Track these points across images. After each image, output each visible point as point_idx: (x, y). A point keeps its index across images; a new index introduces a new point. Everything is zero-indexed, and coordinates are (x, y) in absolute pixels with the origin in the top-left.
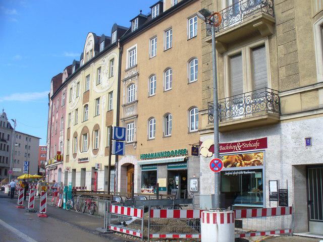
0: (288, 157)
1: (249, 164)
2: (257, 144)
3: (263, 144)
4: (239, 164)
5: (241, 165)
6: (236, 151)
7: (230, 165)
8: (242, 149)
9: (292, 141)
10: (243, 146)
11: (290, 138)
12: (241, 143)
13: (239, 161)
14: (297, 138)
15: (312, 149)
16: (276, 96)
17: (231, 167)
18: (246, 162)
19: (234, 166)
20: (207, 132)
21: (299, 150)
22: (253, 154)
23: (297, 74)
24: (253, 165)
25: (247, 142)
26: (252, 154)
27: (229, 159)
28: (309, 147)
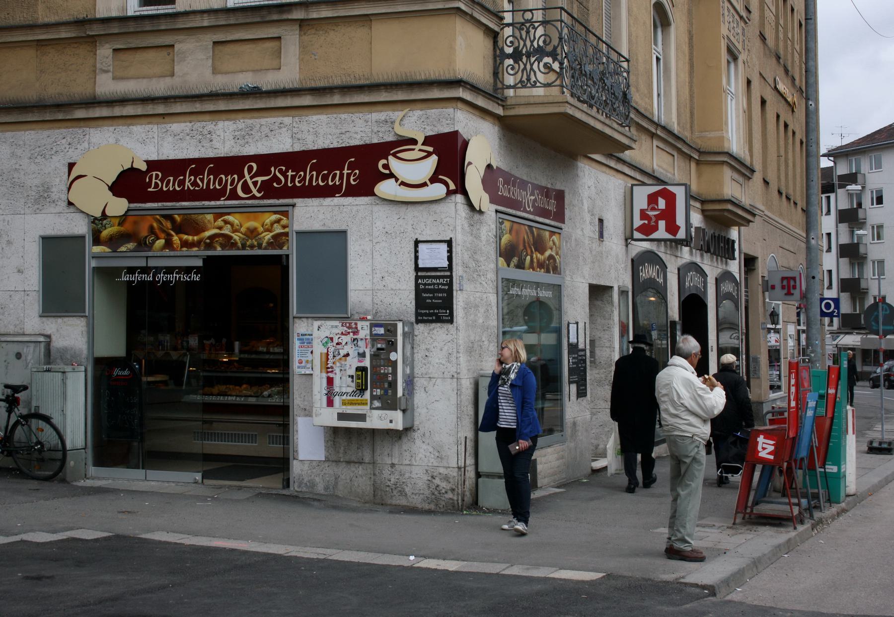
1: (197, 244)
4: (160, 242)
5: (169, 244)
13: (163, 235)
18: (185, 237)
22: (210, 217)
24: (209, 246)
27: (128, 227)
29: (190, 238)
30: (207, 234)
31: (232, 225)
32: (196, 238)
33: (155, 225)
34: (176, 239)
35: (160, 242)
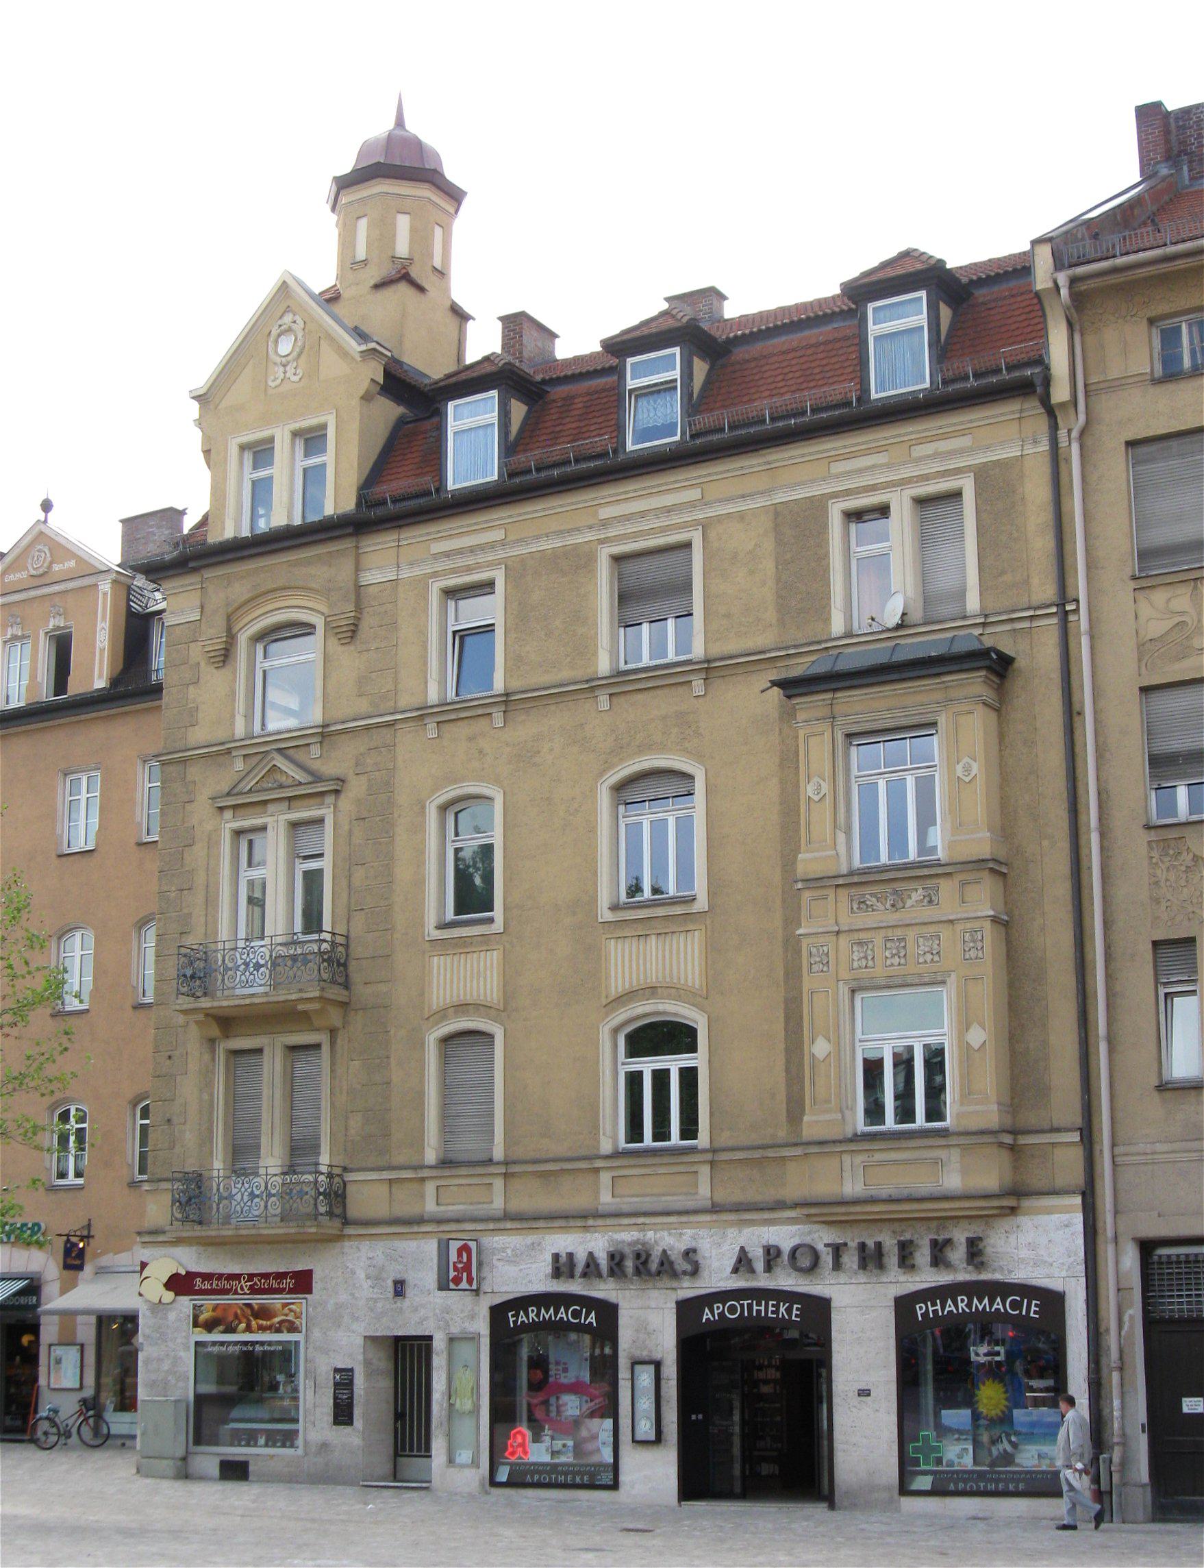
0: (356, 1319)
2: (288, 1283)
3: (303, 1282)
4: (243, 1326)
6: (236, 1293)
7: (221, 1328)
8: (254, 1290)
9: (366, 1284)
10: (255, 1284)
11: (363, 1276)
12: (251, 1276)
13: (245, 1320)
14: (376, 1278)
15: (406, 1303)
16: (337, 1179)
17: (225, 1332)
18: (261, 1322)
19: (231, 1330)
21: (379, 1305)
23: (387, 1135)
24: (278, 1331)
25: (266, 1276)
26: (275, 1302)
27: (219, 1313)
28: (399, 1302)
29: (264, 1323)
30: (277, 1320)
31: (295, 1313)
33: (239, 1312)
34: (254, 1323)
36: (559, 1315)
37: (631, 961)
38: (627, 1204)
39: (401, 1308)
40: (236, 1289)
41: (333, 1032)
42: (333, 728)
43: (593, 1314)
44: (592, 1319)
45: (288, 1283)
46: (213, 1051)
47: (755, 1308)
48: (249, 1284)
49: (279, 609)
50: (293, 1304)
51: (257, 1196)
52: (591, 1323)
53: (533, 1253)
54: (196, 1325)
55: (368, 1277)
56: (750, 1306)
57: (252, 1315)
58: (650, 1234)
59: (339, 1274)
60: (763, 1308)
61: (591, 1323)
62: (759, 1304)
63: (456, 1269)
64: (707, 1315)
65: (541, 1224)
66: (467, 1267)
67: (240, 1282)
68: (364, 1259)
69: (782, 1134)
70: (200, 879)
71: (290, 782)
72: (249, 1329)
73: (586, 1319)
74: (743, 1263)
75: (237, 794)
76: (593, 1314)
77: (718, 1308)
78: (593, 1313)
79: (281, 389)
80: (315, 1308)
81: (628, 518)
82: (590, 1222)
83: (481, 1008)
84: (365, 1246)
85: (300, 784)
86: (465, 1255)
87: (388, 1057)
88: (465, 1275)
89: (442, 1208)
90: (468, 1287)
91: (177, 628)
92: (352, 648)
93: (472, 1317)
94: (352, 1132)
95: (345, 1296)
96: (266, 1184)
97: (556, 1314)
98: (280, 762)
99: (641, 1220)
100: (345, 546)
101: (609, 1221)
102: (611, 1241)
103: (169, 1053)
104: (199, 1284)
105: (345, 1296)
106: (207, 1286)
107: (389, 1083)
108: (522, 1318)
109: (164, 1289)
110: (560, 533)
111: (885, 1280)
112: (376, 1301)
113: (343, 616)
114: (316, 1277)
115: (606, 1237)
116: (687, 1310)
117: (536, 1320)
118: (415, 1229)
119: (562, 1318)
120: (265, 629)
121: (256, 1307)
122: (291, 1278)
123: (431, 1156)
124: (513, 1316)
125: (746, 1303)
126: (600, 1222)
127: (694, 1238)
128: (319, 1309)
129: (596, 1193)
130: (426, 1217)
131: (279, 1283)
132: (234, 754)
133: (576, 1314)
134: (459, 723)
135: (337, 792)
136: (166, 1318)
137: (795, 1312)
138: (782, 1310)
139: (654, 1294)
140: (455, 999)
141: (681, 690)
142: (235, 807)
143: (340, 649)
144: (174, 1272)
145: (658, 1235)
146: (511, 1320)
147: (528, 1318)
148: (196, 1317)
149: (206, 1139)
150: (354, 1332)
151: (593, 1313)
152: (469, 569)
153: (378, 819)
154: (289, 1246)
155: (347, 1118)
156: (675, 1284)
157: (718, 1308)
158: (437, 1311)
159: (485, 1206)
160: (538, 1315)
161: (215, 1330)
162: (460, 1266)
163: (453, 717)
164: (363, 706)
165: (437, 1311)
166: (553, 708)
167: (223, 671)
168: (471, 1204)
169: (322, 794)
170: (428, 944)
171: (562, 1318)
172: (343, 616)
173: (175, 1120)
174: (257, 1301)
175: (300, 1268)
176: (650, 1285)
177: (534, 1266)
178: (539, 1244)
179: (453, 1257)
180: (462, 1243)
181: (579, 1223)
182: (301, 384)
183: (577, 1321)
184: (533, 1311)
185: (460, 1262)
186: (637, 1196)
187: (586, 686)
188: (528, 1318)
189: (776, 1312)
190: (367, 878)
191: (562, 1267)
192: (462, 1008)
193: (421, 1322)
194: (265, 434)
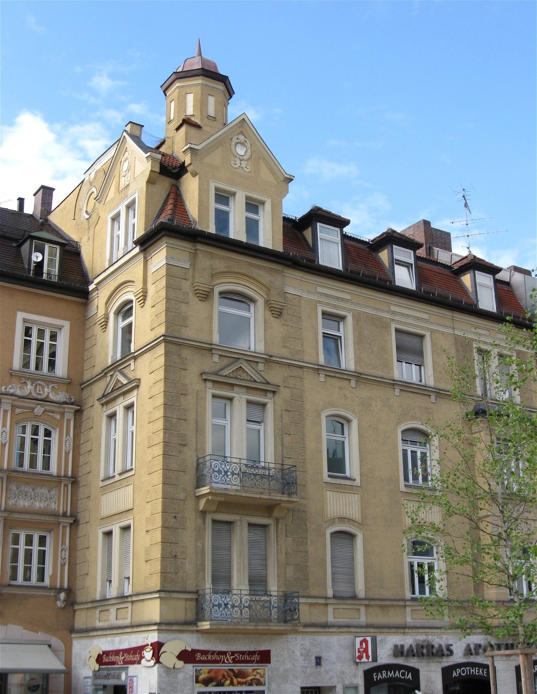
0: (296, 677)
2: (256, 657)
4: (228, 682)
6: (224, 662)
7: (214, 683)
8: (235, 661)
9: (301, 659)
12: (233, 653)
13: (229, 679)
14: (306, 655)
15: (322, 669)
18: (239, 680)
20: (175, 628)
21: (308, 670)
23: (307, 579)
24: (251, 684)
25: (243, 653)
26: (248, 668)
27: (212, 675)
28: (318, 667)
30: (249, 678)
31: (260, 674)
32: (244, 680)
33: (225, 673)
34: (235, 680)
35: (228, 682)
36: (396, 675)
37: (340, 506)
38: (418, 623)
39: (320, 672)
40: (224, 661)
41: (277, 520)
42: (274, 359)
43: (410, 674)
44: (410, 676)
45: (256, 657)
46: (204, 519)
47: (471, 671)
48: (232, 657)
49: (246, 286)
50: (259, 669)
51: (247, 607)
52: (409, 678)
53: (382, 645)
54: (197, 681)
55: (301, 655)
56: (470, 670)
57: (234, 676)
58: (430, 637)
59: (286, 653)
60: (474, 671)
61: (409, 678)
62: (473, 669)
63: (359, 651)
64: (454, 674)
65: (386, 630)
66: (366, 650)
67: (226, 656)
68: (299, 645)
69: (473, 595)
70: (192, 416)
71: (249, 378)
72: (232, 684)
73: (407, 676)
74: (468, 651)
75: (220, 375)
76: (410, 674)
77: (458, 671)
78: (410, 674)
79: (235, 170)
80: (272, 671)
81: (403, 315)
82: (407, 630)
83: (351, 521)
84: (299, 637)
85: (255, 381)
86: (364, 644)
87: (306, 538)
88: (364, 654)
89: (336, 620)
90: (366, 660)
91: (174, 267)
92: (278, 320)
93: (355, 676)
94: (288, 575)
95: (289, 665)
96: (241, 599)
97: (395, 674)
98: (246, 366)
99: (426, 630)
100: (279, 269)
101: (414, 631)
102: (415, 640)
103: (174, 515)
104: (198, 656)
105: (289, 665)
106: (204, 658)
107: (307, 552)
108: (380, 676)
109: (176, 659)
110: (375, 309)
111: (511, 659)
112: (306, 668)
113: (280, 304)
114: (272, 654)
115: (413, 638)
116: (447, 672)
117: (386, 677)
118: (327, 630)
119: (397, 676)
120: (241, 292)
121: (236, 671)
122: (258, 654)
123: (330, 593)
124: (375, 675)
125: (468, 668)
126: (410, 631)
127: (446, 639)
128: (275, 672)
129: (405, 616)
130: (329, 624)
131: (250, 658)
132: (213, 352)
133: (403, 674)
134: (334, 379)
135: (274, 392)
136: (177, 678)
137: (485, 672)
138: (481, 671)
139: (433, 664)
140: (335, 515)
141: (426, 397)
142: (214, 382)
143: (272, 318)
144: (184, 649)
145: (433, 638)
146: (375, 677)
147: (382, 676)
148: (197, 677)
149: (201, 568)
150: (295, 685)
151: (410, 674)
152: (335, 307)
153: (297, 413)
154: (256, 636)
155: (285, 568)
156: (440, 660)
157: (458, 671)
158: (338, 673)
159: (357, 620)
160: (387, 675)
161: (210, 685)
162: (361, 650)
163: (333, 375)
164: (285, 352)
165: (338, 673)
166: (376, 386)
167: (203, 303)
168: (350, 618)
169: (266, 391)
170: (324, 484)
171: (397, 676)
172: (280, 304)
173: (179, 556)
174: (237, 667)
175: (263, 648)
176: (431, 661)
177: (382, 650)
178: (384, 640)
179: (358, 646)
180: (363, 638)
181: (402, 631)
182: (249, 174)
183: (403, 677)
184: (384, 673)
185: (362, 648)
186: (421, 619)
187: (392, 382)
188: (382, 676)
189: (479, 672)
190: (292, 442)
191: (398, 651)
192: (342, 519)
193: (331, 678)
194: (233, 189)
